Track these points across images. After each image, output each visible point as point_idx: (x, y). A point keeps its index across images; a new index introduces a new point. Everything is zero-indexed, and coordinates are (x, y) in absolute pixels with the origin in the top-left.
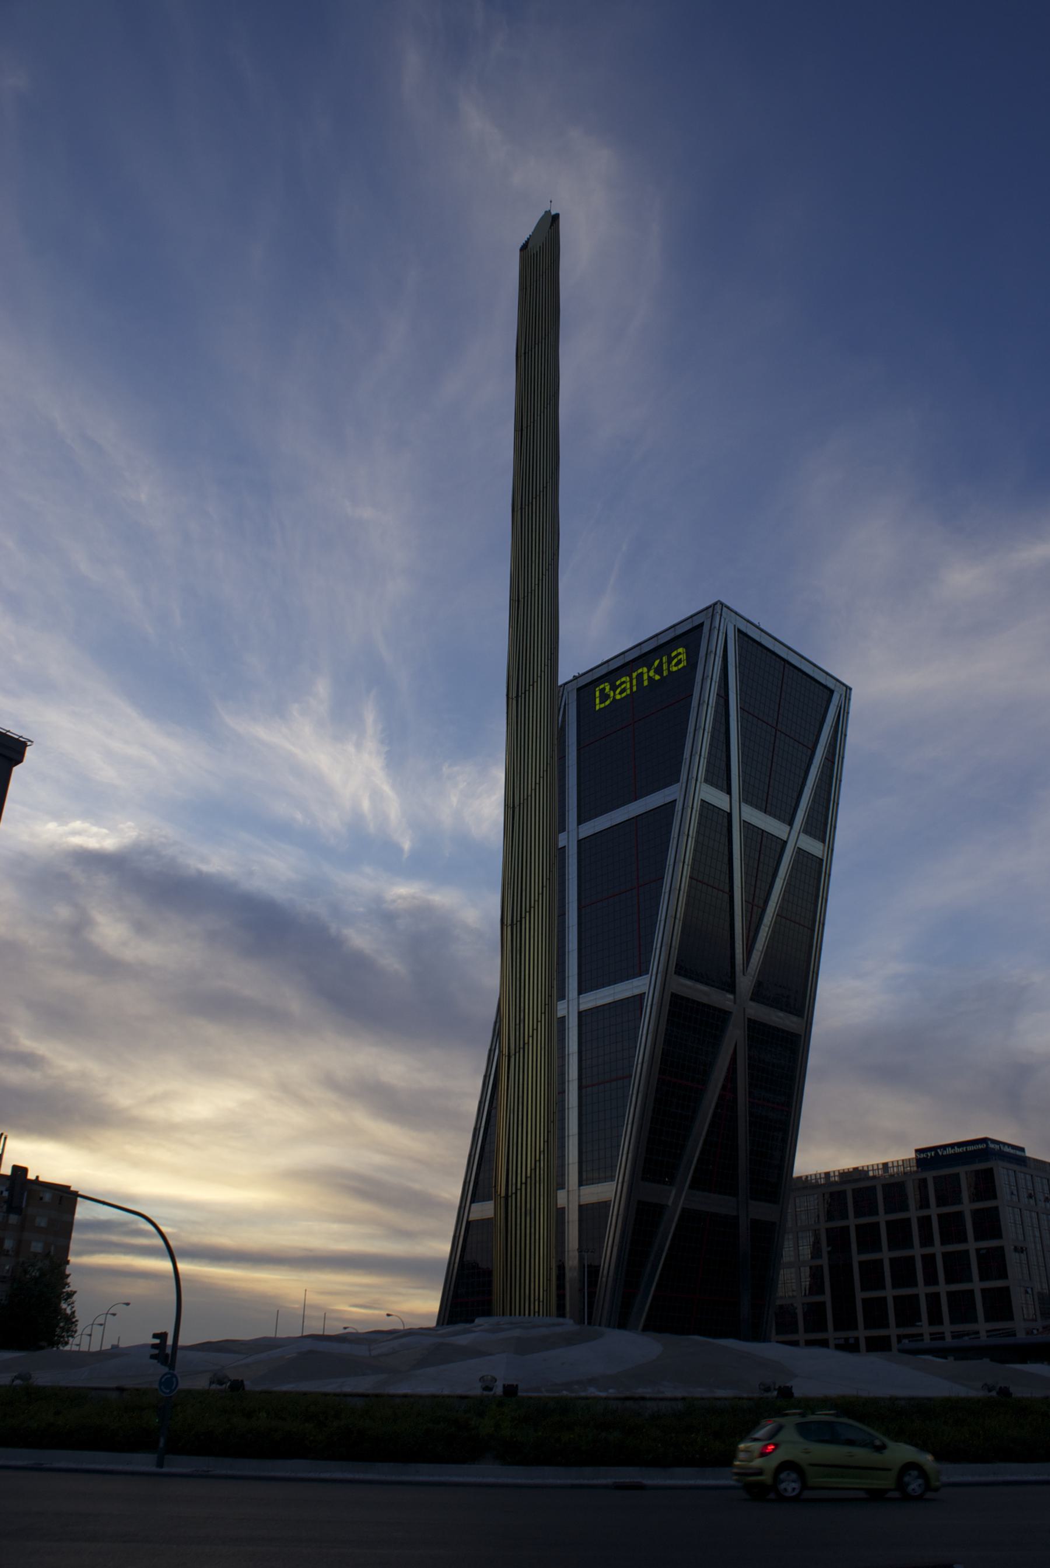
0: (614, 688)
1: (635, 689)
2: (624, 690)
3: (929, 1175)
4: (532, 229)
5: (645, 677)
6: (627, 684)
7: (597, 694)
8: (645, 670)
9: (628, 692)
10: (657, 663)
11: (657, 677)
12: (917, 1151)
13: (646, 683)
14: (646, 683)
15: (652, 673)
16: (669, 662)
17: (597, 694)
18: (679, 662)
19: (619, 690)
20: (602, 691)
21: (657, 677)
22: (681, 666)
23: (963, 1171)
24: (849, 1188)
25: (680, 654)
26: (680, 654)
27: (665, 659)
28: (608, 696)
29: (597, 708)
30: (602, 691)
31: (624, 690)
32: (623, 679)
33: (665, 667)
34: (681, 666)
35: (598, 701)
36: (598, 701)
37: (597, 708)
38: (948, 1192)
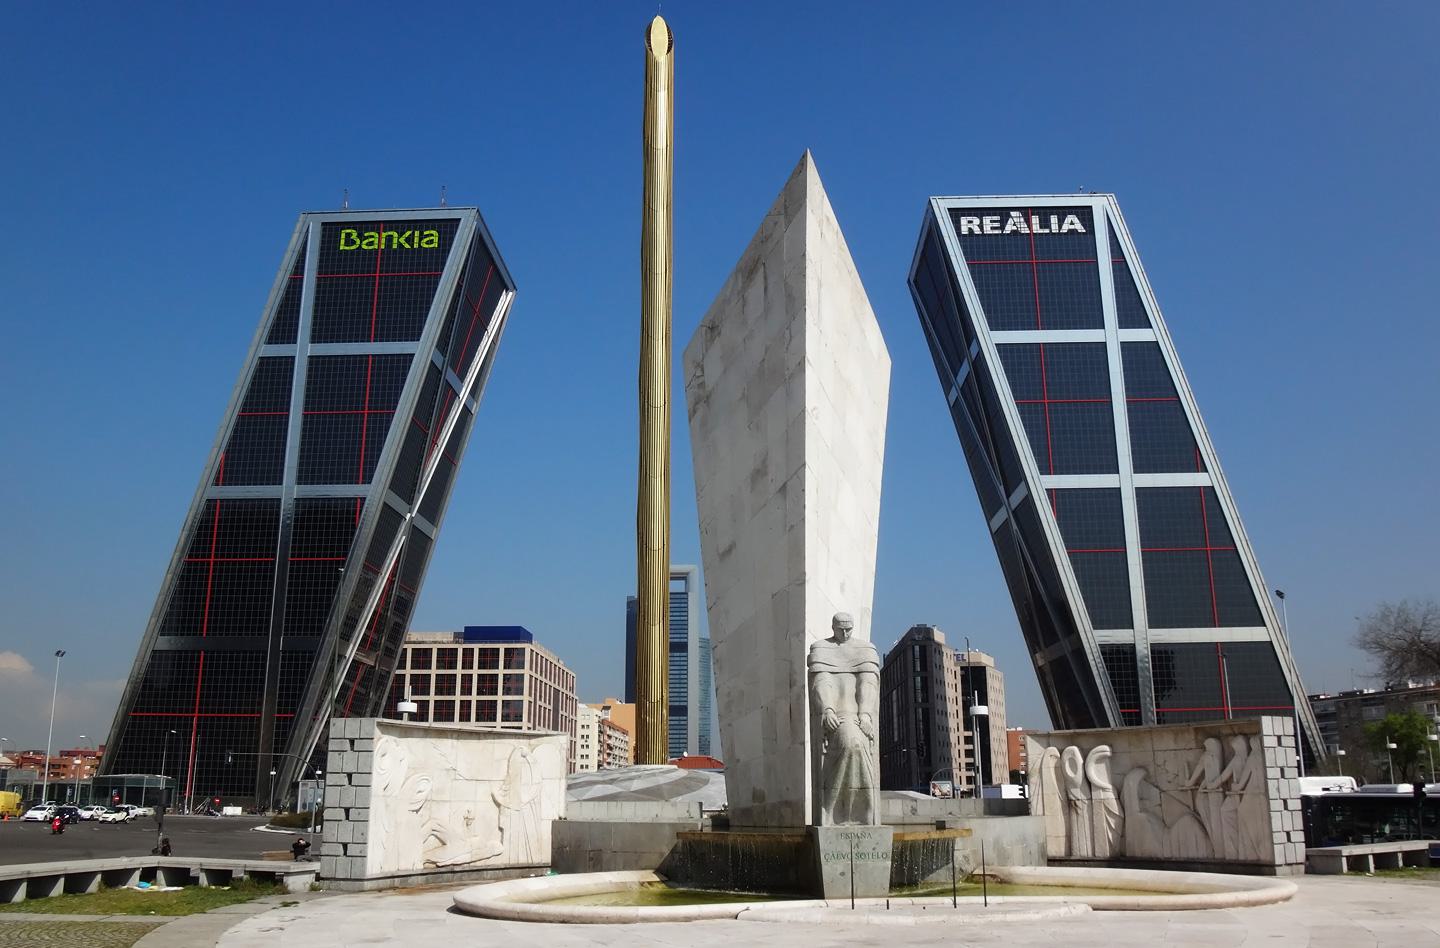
0: (361, 236)
1: (383, 247)
2: (371, 243)
3: (476, 647)
4: (876, 322)
5: (395, 241)
6: (375, 241)
7: (343, 236)
8: (396, 235)
9: (376, 247)
10: (408, 233)
11: (407, 246)
12: (466, 628)
13: (395, 246)
14: (395, 246)
15: (402, 240)
16: (421, 239)
17: (343, 236)
18: (431, 242)
19: (366, 241)
20: (348, 235)
21: (407, 246)
22: (431, 246)
23: (502, 647)
24: (409, 648)
25: (432, 235)
26: (432, 235)
27: (417, 233)
28: (354, 243)
29: (342, 248)
30: (348, 235)
31: (371, 243)
32: (372, 234)
33: (416, 240)
34: (431, 246)
35: (343, 242)
36: (343, 242)
37: (342, 248)
38: (489, 659)
